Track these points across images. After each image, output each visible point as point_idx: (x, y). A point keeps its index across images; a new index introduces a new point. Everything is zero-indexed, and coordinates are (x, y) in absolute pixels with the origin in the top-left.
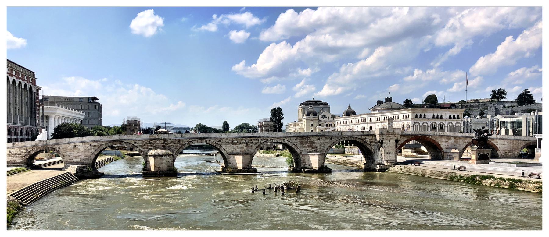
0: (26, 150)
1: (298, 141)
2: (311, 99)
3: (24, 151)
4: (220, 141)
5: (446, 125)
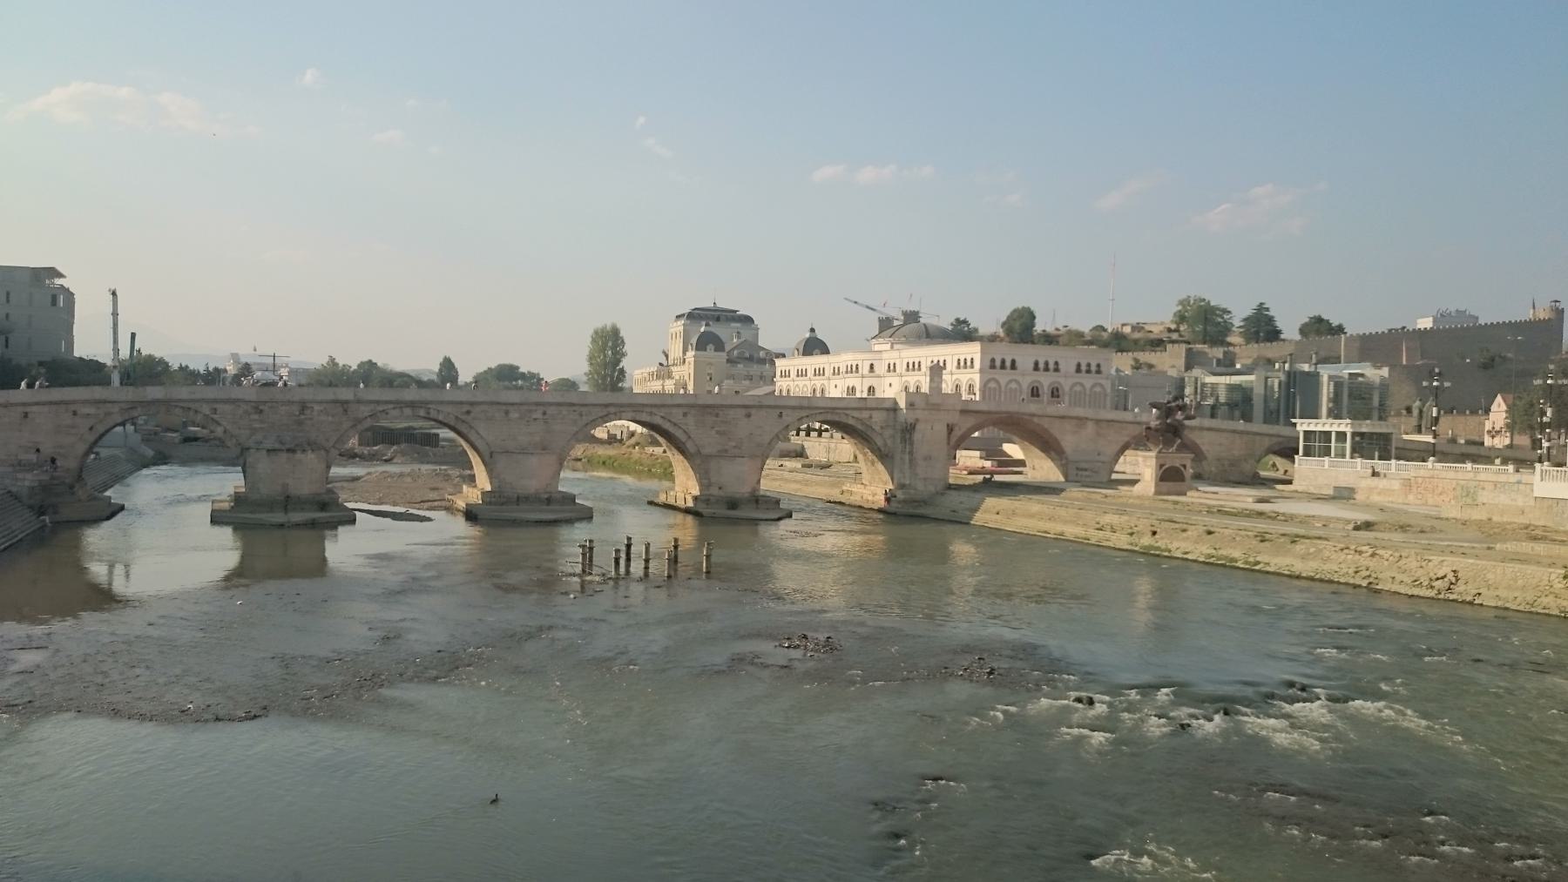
1: (690, 420)
4: (468, 412)
5: (1067, 389)
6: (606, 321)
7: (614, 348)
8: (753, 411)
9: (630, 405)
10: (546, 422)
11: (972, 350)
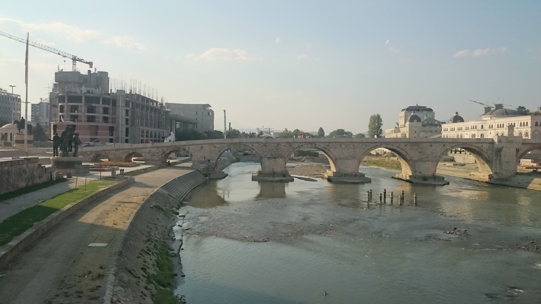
0: (163, 150)
2: (414, 105)
3: (161, 150)
6: (375, 113)
7: (379, 121)
8: (433, 144)
9: (384, 142)
10: (354, 149)
11: (527, 119)
